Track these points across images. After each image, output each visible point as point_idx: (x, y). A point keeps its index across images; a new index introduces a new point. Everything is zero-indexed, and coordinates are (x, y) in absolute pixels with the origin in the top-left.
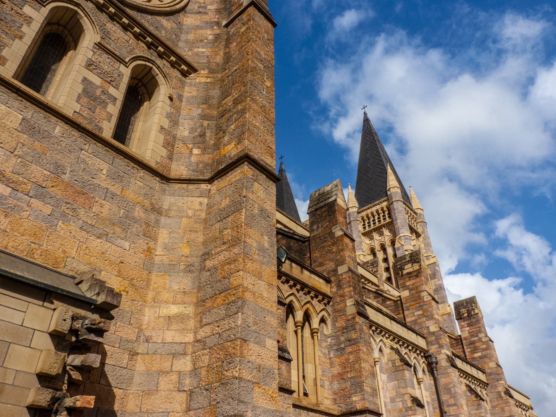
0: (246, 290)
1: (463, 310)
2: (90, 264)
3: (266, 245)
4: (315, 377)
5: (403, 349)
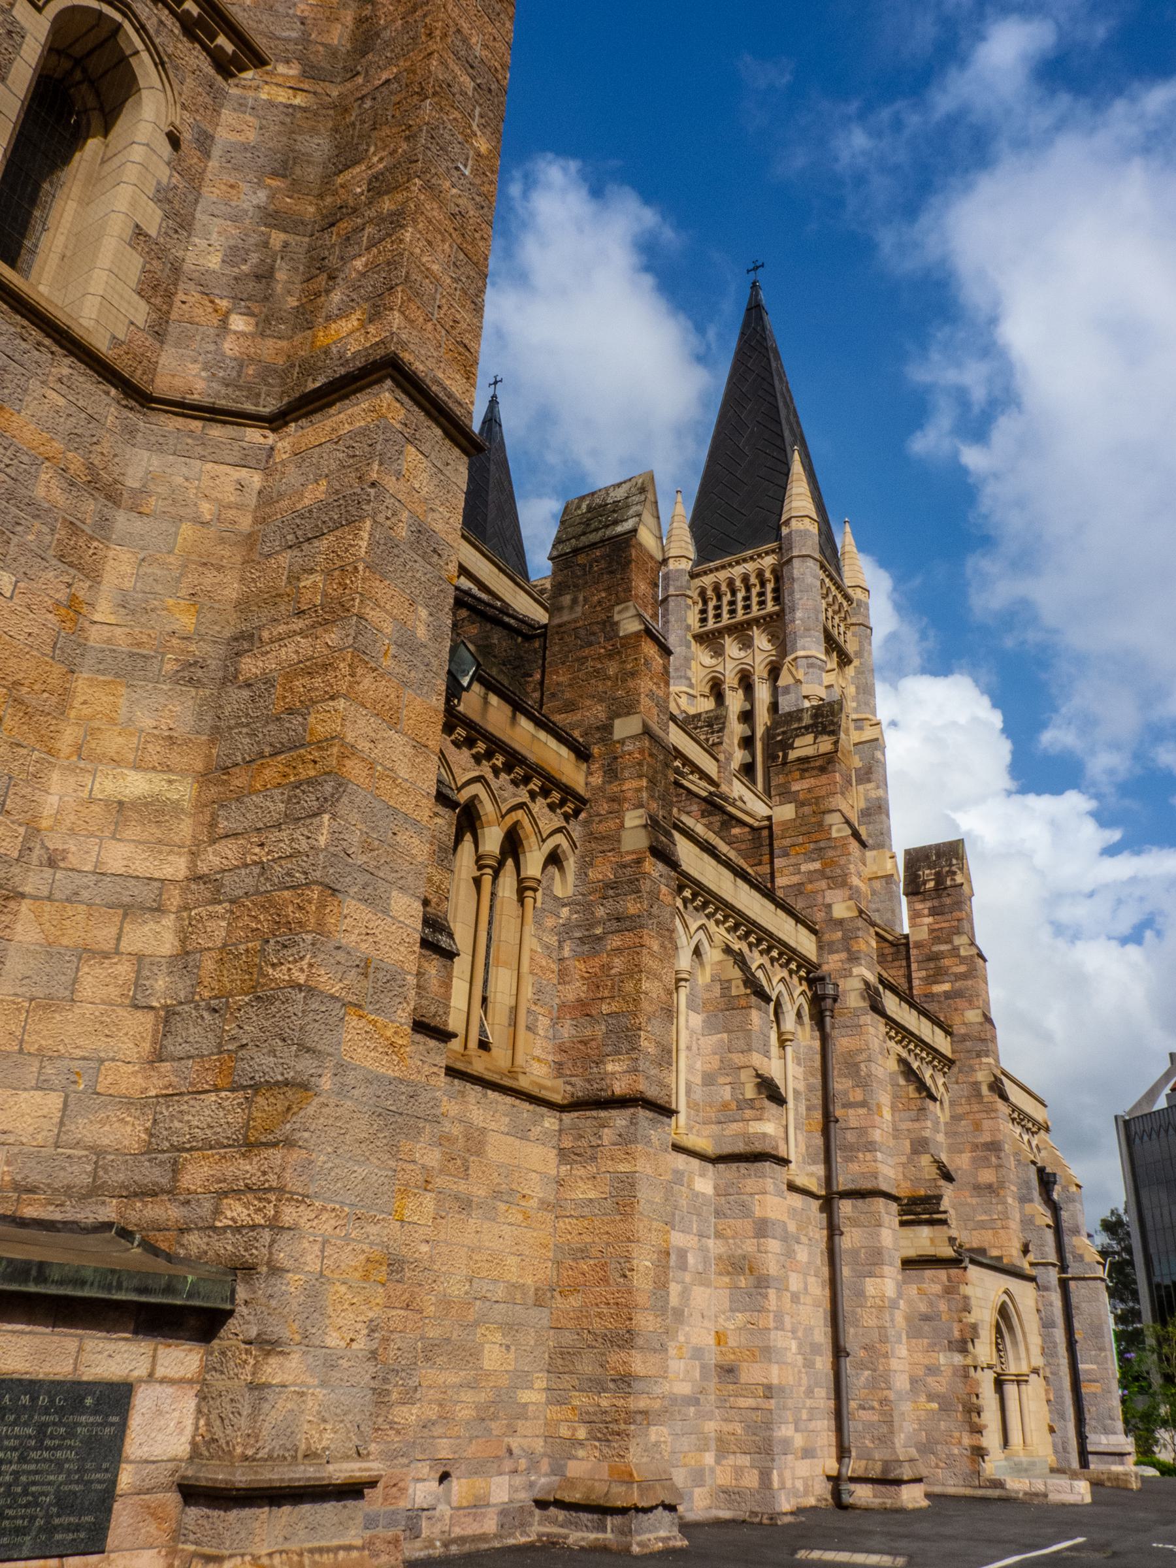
0: (349, 751)
1: (927, 873)
3: (422, 633)
4: (513, 1003)
5: (756, 954)
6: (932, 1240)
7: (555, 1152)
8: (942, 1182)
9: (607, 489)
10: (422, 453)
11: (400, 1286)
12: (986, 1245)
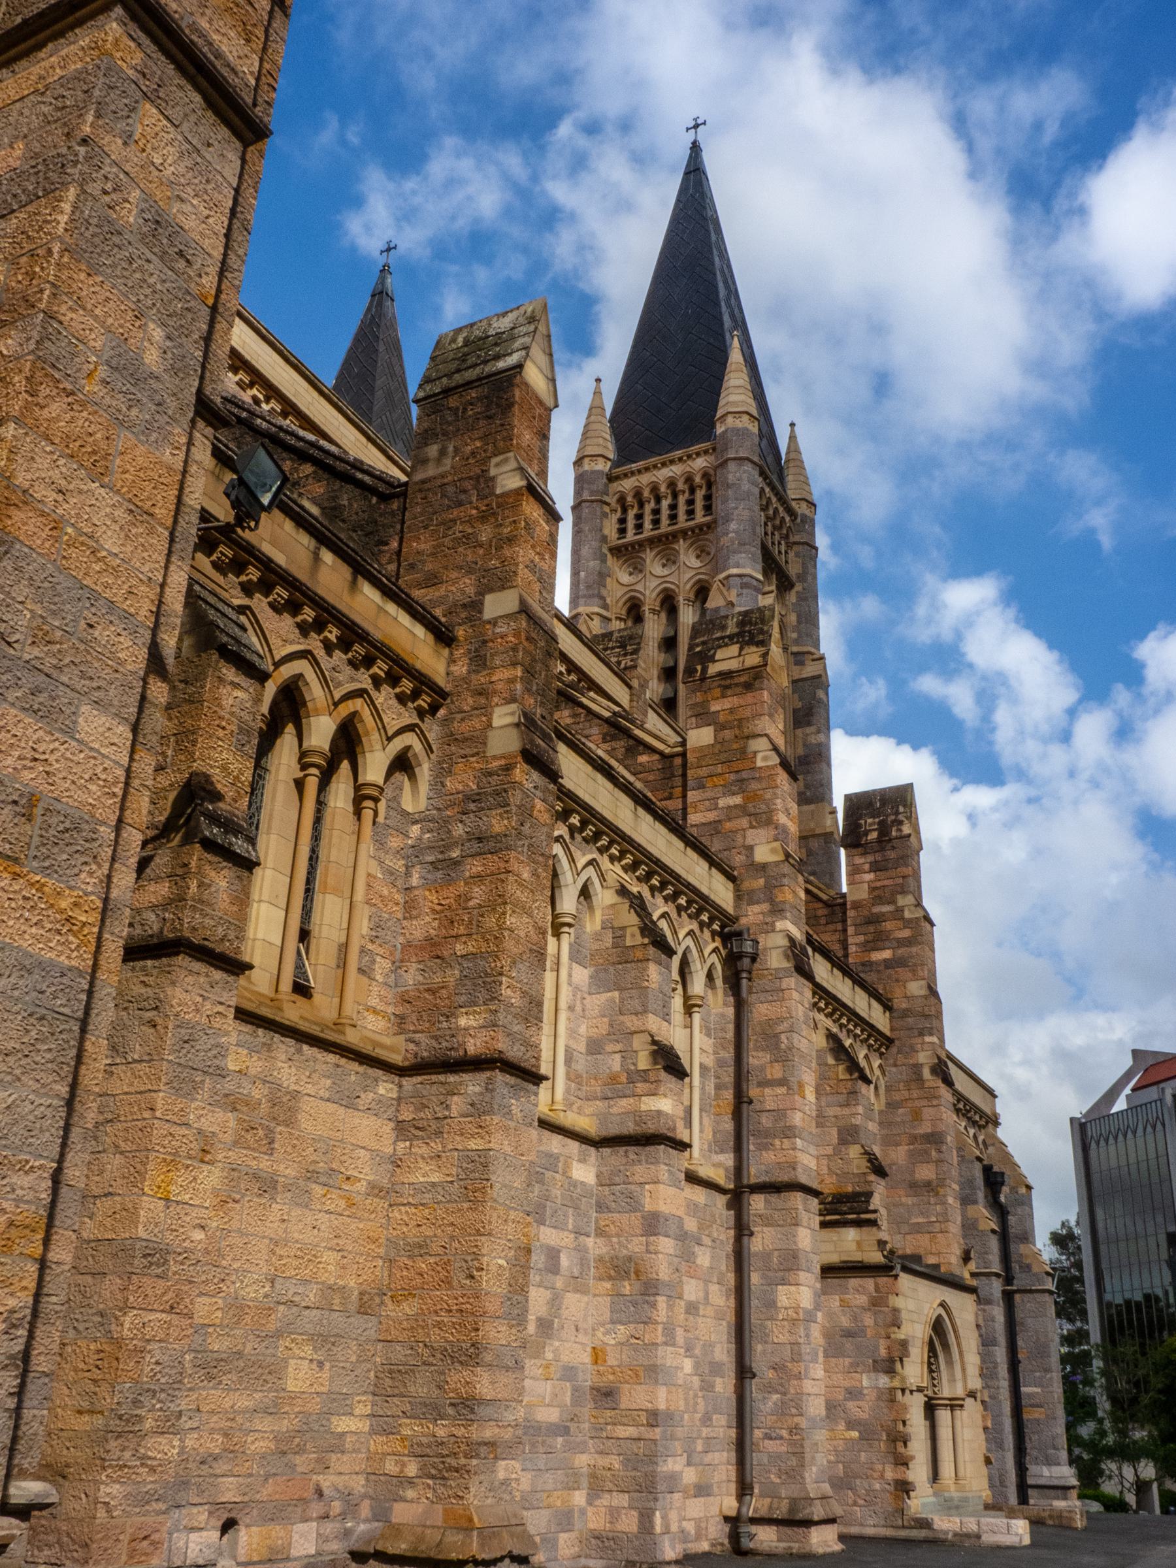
1: (870, 822)
3: (152, 358)
4: (343, 939)
5: (659, 900)
6: (859, 1243)
7: (392, 1125)
8: (872, 1177)
9: (489, 319)
10: (167, 118)
11: (161, 1282)
12: (921, 1251)
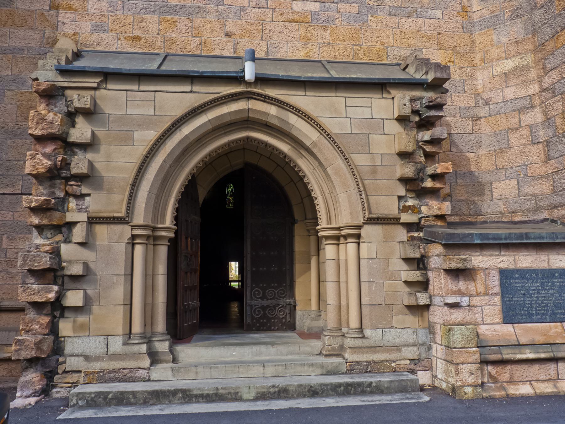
2: (409, 46)
